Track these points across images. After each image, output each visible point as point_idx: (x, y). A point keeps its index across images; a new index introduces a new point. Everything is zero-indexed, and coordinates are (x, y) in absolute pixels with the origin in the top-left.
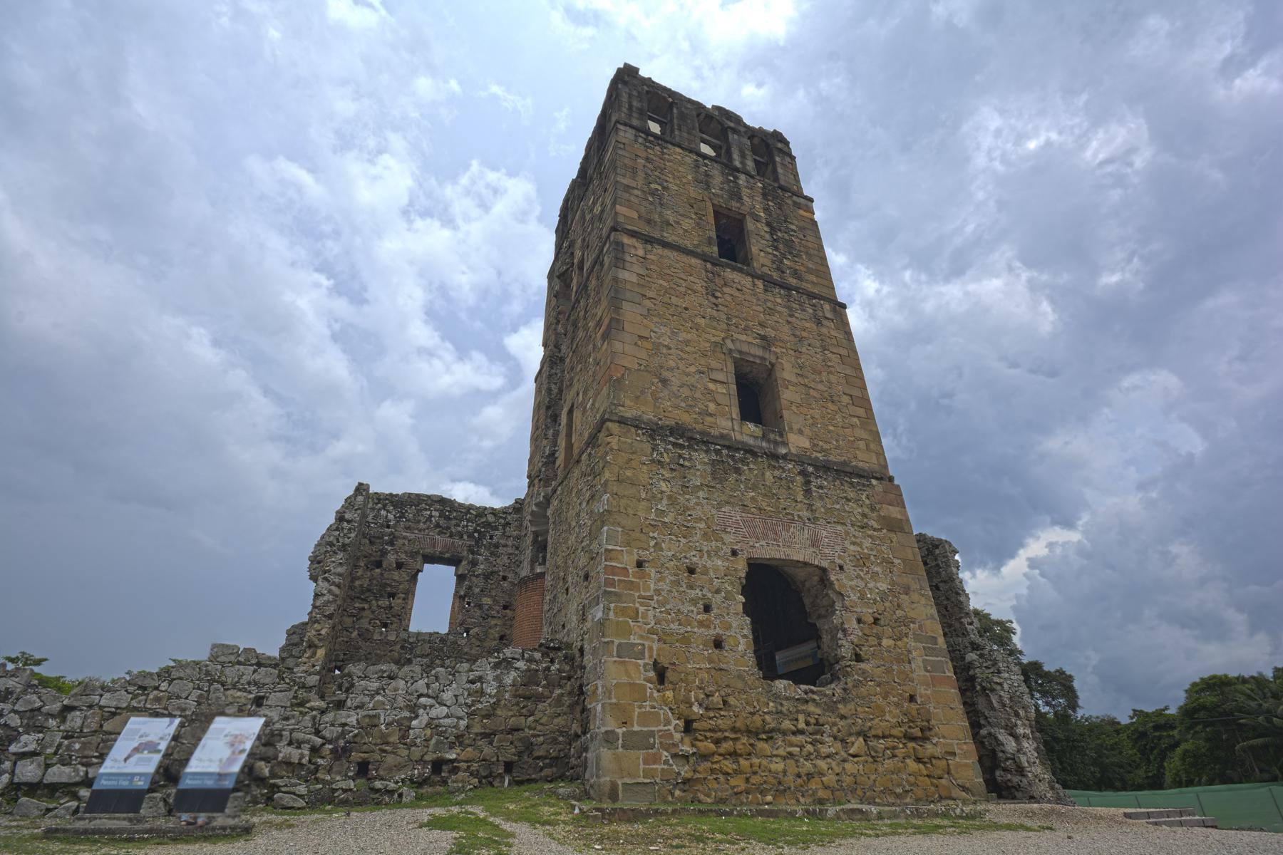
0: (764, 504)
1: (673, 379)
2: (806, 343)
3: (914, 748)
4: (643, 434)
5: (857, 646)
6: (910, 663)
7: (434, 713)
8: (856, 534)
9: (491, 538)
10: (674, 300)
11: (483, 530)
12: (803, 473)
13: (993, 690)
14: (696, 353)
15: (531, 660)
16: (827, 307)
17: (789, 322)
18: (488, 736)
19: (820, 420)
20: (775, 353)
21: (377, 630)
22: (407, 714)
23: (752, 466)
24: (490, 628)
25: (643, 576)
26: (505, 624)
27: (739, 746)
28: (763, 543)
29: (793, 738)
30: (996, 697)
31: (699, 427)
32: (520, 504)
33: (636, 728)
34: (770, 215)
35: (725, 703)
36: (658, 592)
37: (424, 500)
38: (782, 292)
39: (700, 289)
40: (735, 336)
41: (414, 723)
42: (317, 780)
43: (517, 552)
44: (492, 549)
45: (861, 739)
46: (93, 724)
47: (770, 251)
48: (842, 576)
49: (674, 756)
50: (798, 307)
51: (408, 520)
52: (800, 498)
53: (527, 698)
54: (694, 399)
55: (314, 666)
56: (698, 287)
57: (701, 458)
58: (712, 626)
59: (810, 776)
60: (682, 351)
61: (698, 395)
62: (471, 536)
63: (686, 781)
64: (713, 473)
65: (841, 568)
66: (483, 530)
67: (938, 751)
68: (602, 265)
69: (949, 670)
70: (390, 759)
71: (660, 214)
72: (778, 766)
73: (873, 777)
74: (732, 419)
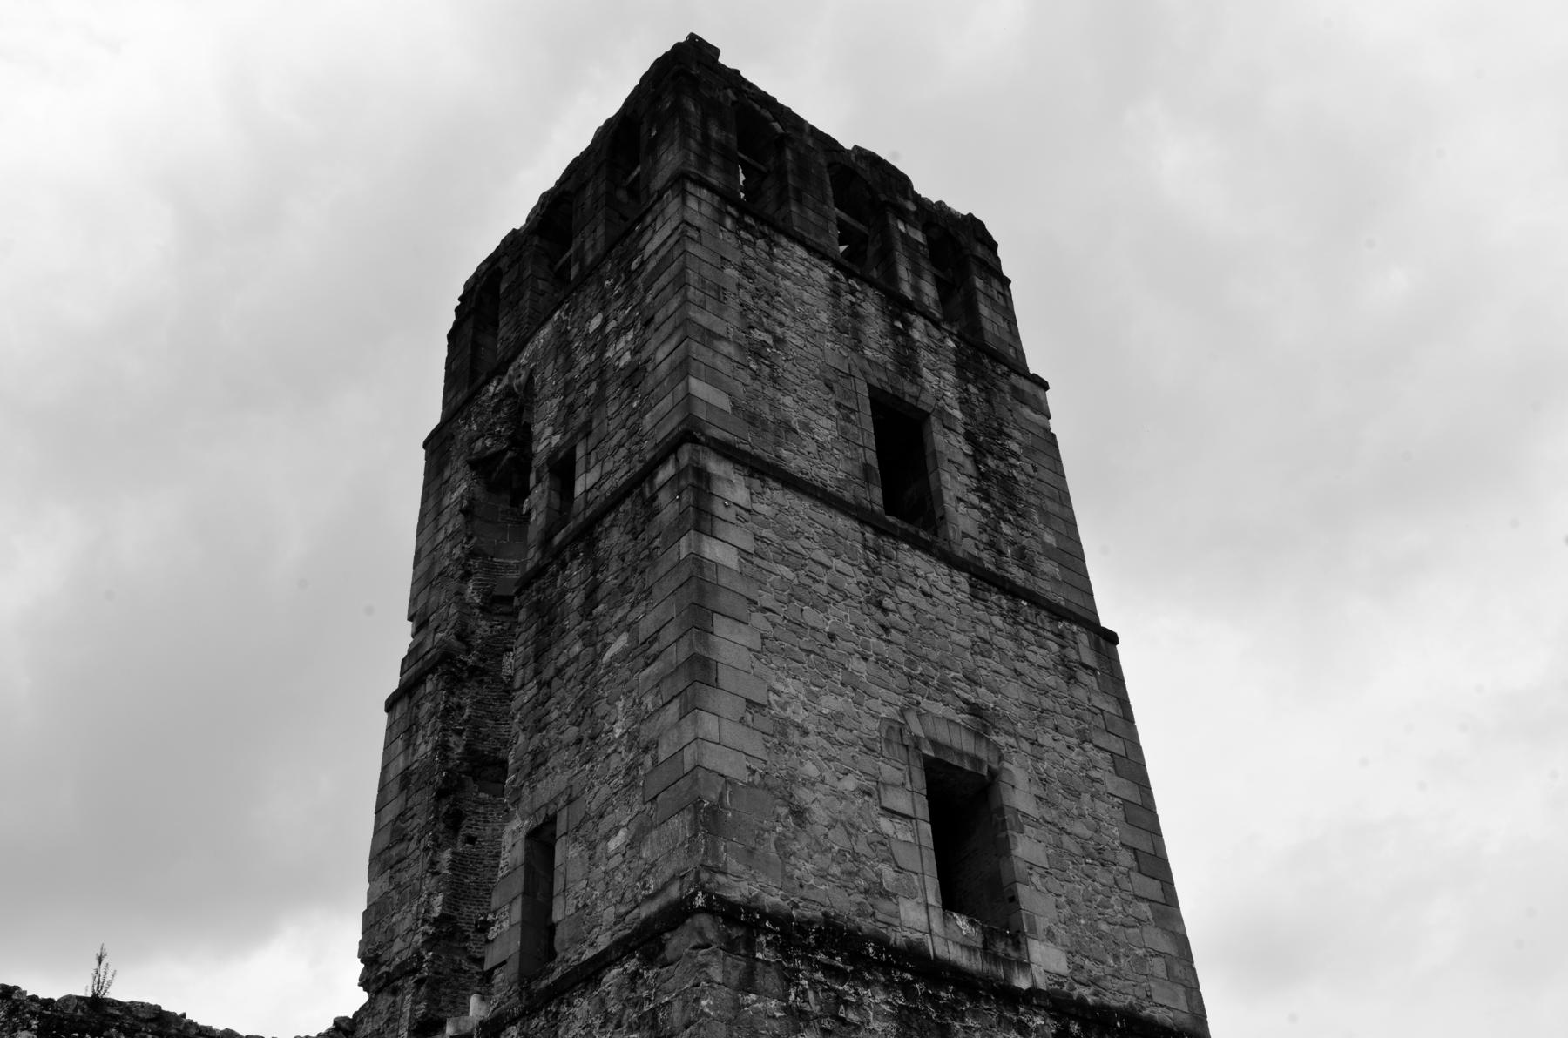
1: (814, 807)
2: (1049, 723)
4: (769, 944)
10: (811, 616)
14: (852, 744)
16: (1084, 639)
17: (1018, 673)
19: (1084, 910)
20: (997, 747)
23: (970, 1022)
31: (867, 925)
34: (972, 416)
37: (115, 1018)
39: (855, 590)
40: (925, 703)
47: (974, 499)
50: (1031, 637)
54: (856, 856)
56: (850, 585)
60: (828, 738)
61: (862, 848)
68: (650, 507)
71: (774, 405)
74: (927, 906)
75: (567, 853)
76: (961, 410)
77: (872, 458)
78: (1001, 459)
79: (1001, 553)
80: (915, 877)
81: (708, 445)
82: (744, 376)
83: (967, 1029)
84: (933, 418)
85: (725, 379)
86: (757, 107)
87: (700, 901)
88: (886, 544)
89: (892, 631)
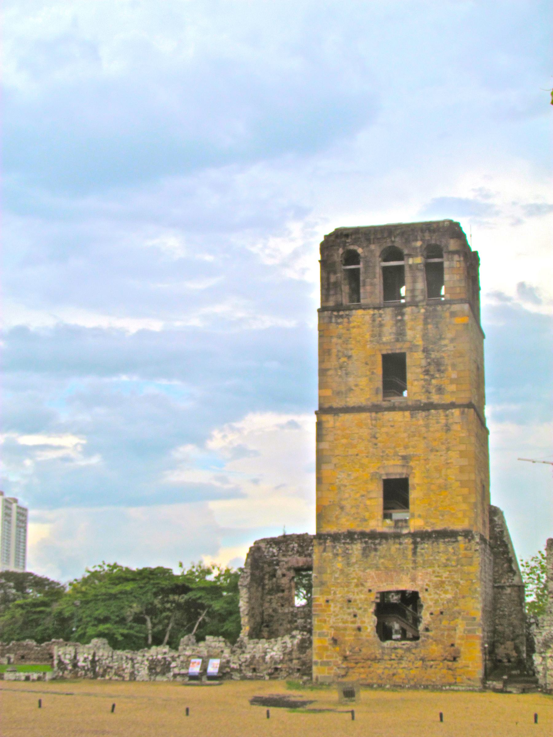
5: (428, 625)
6: (455, 630)
12: (415, 543)
15: (303, 635)
25: (328, 606)
27: (364, 665)
28: (385, 584)
29: (389, 662)
31: (359, 529)
33: (325, 659)
36: (334, 612)
38: (424, 414)
46: (186, 660)
47: (422, 376)
49: (339, 668)
51: (283, 551)
53: (302, 647)
54: (358, 513)
57: (357, 548)
59: (394, 675)
60: (353, 485)
64: (363, 554)
72: (380, 671)
74: (378, 520)
76: (423, 340)
78: (438, 351)
79: (430, 393)
83: (383, 548)
86: (352, 247)
88: (380, 415)
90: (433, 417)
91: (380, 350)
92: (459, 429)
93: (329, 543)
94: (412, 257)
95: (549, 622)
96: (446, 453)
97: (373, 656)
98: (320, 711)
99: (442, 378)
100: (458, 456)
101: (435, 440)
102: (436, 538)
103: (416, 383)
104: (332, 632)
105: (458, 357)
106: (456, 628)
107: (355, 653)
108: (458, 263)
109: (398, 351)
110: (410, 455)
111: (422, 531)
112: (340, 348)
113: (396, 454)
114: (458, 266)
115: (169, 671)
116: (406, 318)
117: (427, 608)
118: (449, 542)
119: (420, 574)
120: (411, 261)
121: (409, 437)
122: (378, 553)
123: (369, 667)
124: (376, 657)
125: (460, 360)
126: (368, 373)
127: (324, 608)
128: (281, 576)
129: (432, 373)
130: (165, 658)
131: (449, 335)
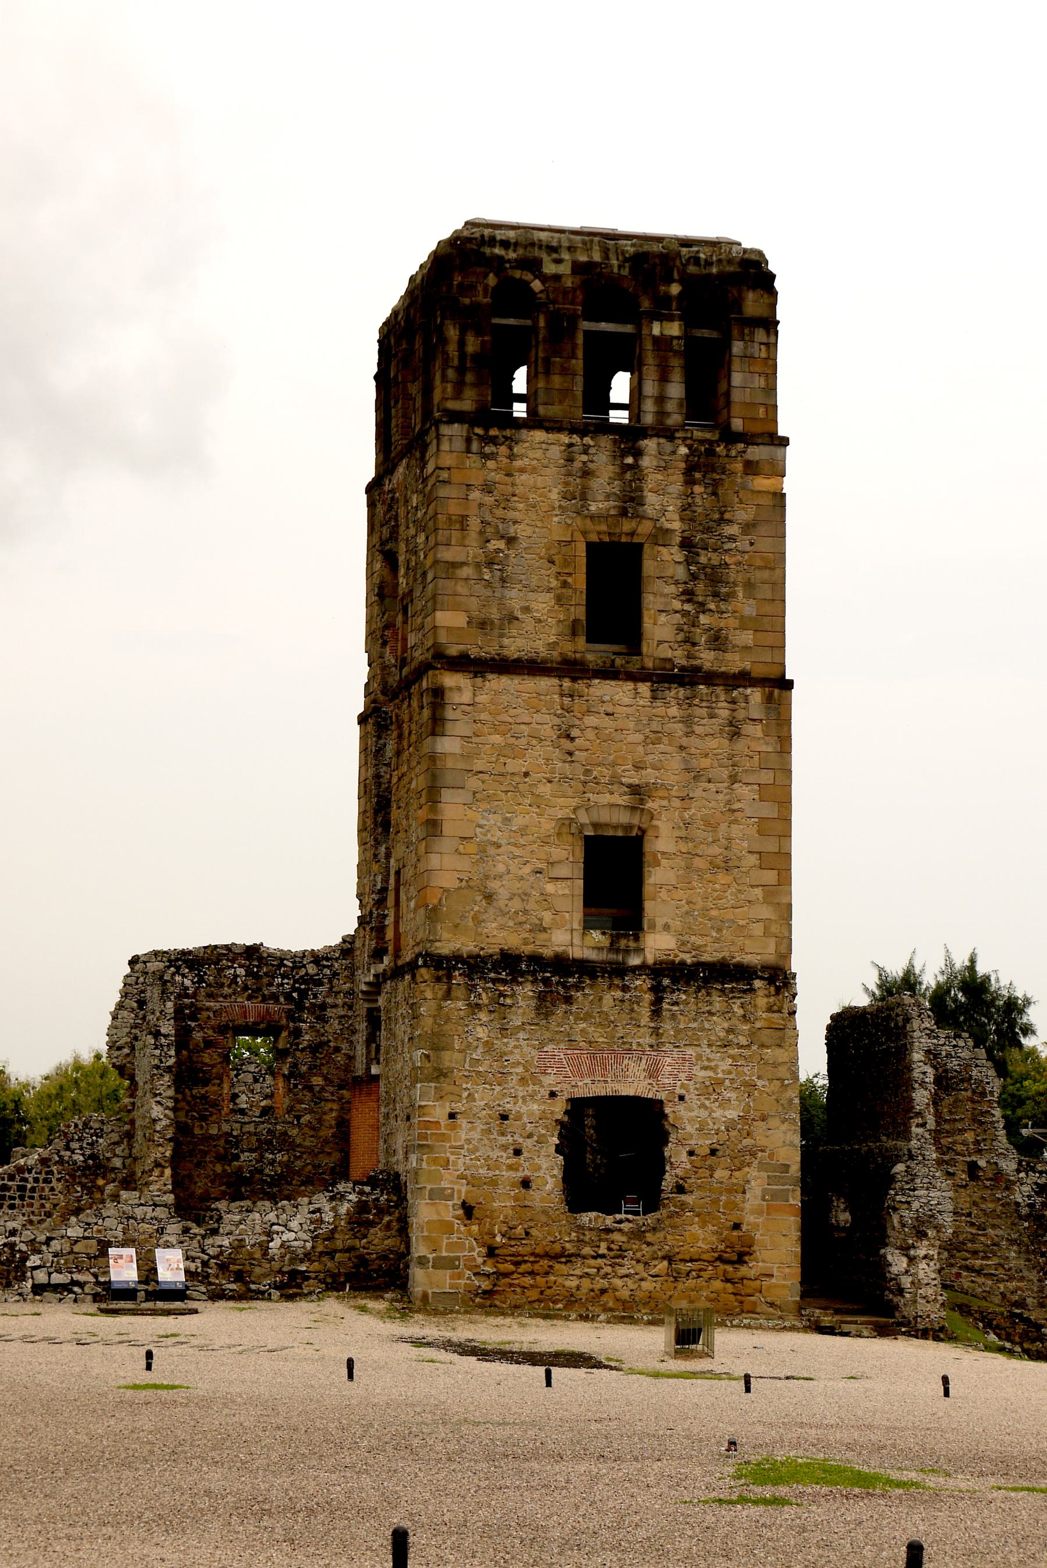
0: (596, 1035)
1: (501, 891)
3: (725, 1271)
4: (460, 975)
6: (744, 1192)
7: (285, 1237)
8: (710, 1056)
9: (315, 996)
11: (303, 987)
12: (657, 990)
13: (895, 1209)
15: (361, 1193)
18: (331, 1254)
21: (197, 1124)
22: (265, 1238)
24: (325, 1113)
25: (453, 1128)
26: (342, 1109)
27: (536, 1267)
28: (588, 1081)
29: (592, 1262)
30: (898, 1216)
31: (528, 949)
32: (350, 943)
33: (444, 1254)
35: (527, 1234)
36: (468, 1141)
37: (224, 955)
38: (682, 692)
41: (271, 1244)
42: (211, 1284)
43: (350, 1013)
44: (318, 1013)
45: (665, 1263)
46: (67, 1248)
47: (677, 605)
48: (681, 1107)
49: (475, 1274)
51: (209, 985)
52: (645, 1019)
54: (525, 912)
55: (165, 1185)
57: (525, 992)
58: (521, 1169)
59: (603, 1291)
60: (515, 845)
62: (288, 997)
63: (485, 1292)
64: (537, 1009)
65: (682, 1098)
66: (303, 987)
67: (752, 1273)
69: (794, 1199)
70: (257, 1270)
72: (572, 1283)
73: (669, 1293)
74: (572, 931)
75: (403, 897)
76: (682, 519)
77: (580, 612)
78: (715, 550)
79: (694, 644)
80: (567, 914)
81: (443, 668)
82: (479, 589)
84: (646, 546)
85: (463, 599)
86: (518, 274)
87: (420, 963)
88: (580, 686)
89: (577, 753)
90: (702, 700)
91: (584, 533)
92: (760, 734)
93: (458, 979)
94: (661, 322)
95: (926, 1180)
96: (728, 788)
97: (557, 1248)
98: (718, 1376)
99: (723, 612)
100: (756, 797)
101: (706, 755)
102: (706, 981)
103: (663, 618)
104: (463, 1190)
105: (760, 568)
106: (747, 1186)
107: (515, 1239)
108: (762, 347)
109: (624, 539)
110: (647, 784)
111: (673, 962)
112: (489, 518)
113: (615, 780)
114: (764, 355)
115: (23, 1278)
116: (646, 462)
117: (680, 1143)
118: (732, 990)
119: (669, 1060)
120: (656, 329)
121: (645, 742)
122: (574, 1008)
123: (547, 1273)
124: (563, 1248)
125: (765, 574)
126: (554, 583)
127: (443, 1131)
128: (202, 1045)
129: (700, 599)
130: (12, 1246)
131: (743, 515)
